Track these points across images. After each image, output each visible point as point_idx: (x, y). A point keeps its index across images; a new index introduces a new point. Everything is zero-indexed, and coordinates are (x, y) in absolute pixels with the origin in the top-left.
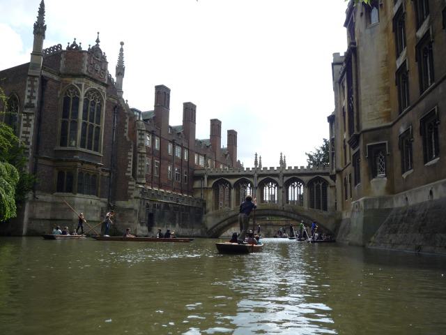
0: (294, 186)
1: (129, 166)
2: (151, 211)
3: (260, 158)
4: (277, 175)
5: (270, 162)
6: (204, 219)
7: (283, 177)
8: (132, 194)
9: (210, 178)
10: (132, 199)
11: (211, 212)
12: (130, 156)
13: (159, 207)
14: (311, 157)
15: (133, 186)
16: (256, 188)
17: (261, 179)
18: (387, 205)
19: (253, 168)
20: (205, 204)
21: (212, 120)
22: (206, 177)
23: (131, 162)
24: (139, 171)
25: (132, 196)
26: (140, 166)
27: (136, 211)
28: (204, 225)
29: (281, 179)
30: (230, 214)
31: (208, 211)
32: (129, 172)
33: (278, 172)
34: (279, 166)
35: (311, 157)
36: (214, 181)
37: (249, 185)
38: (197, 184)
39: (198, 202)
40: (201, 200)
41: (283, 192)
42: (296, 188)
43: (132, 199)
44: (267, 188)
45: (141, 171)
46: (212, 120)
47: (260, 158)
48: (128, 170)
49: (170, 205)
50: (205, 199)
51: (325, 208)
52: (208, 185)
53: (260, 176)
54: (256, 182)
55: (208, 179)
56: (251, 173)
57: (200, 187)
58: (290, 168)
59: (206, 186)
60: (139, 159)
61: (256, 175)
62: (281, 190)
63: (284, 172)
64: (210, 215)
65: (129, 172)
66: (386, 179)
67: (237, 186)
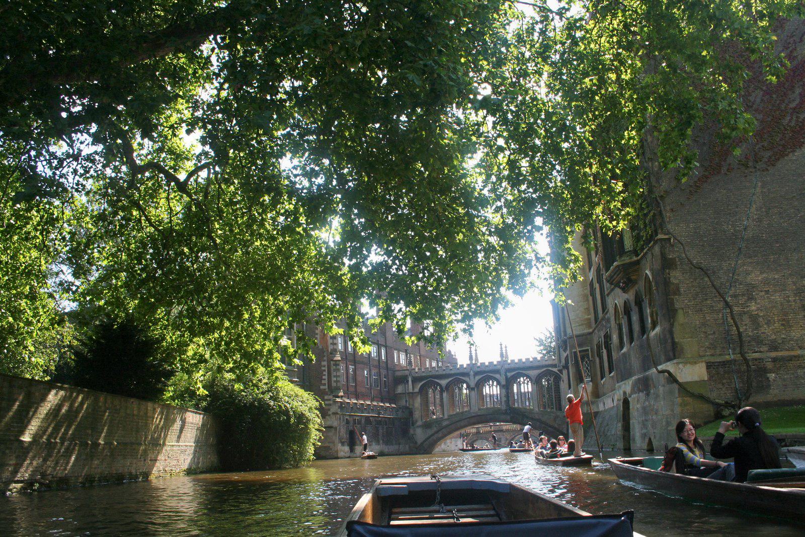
0: (519, 382)
1: (324, 377)
2: (351, 428)
6: (412, 432)
8: (329, 410)
9: (416, 380)
10: (329, 415)
12: (324, 366)
13: (359, 423)
14: (541, 343)
15: (330, 400)
17: (478, 378)
18: (594, 409)
19: (468, 365)
20: (411, 413)
23: (326, 373)
24: (334, 381)
25: (330, 413)
26: (334, 376)
27: (336, 428)
28: (412, 439)
30: (445, 424)
31: (417, 421)
32: (324, 385)
33: (499, 367)
35: (541, 343)
36: (421, 384)
37: (465, 386)
38: (400, 389)
39: (403, 412)
40: (407, 408)
43: (329, 415)
44: (487, 387)
45: (337, 382)
48: (323, 382)
49: (371, 418)
50: (411, 407)
52: (413, 389)
53: (476, 374)
56: (465, 371)
59: (411, 391)
60: (333, 368)
61: (472, 373)
63: (506, 366)
64: (418, 427)
65: (324, 385)
66: (591, 383)
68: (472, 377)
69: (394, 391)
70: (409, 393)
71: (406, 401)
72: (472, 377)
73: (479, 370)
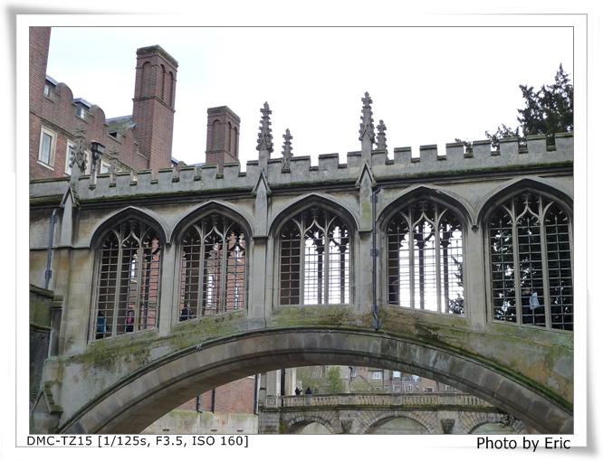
3: (288, 137)
4: (349, 186)
9: (85, 208)
16: (262, 241)
17: (281, 205)
22: (68, 207)
31: (70, 342)
33: (354, 172)
34: (357, 146)
41: (375, 253)
47: (288, 137)
50: (57, 293)
52: (75, 237)
53: (276, 192)
54: (260, 217)
55: (75, 211)
56: (242, 184)
57: (46, 246)
58: (403, 151)
59: (66, 240)
61: (262, 191)
63: (380, 170)
64: (73, 359)
67: (186, 236)
70: (59, 249)
71: (49, 274)
73: (286, 180)
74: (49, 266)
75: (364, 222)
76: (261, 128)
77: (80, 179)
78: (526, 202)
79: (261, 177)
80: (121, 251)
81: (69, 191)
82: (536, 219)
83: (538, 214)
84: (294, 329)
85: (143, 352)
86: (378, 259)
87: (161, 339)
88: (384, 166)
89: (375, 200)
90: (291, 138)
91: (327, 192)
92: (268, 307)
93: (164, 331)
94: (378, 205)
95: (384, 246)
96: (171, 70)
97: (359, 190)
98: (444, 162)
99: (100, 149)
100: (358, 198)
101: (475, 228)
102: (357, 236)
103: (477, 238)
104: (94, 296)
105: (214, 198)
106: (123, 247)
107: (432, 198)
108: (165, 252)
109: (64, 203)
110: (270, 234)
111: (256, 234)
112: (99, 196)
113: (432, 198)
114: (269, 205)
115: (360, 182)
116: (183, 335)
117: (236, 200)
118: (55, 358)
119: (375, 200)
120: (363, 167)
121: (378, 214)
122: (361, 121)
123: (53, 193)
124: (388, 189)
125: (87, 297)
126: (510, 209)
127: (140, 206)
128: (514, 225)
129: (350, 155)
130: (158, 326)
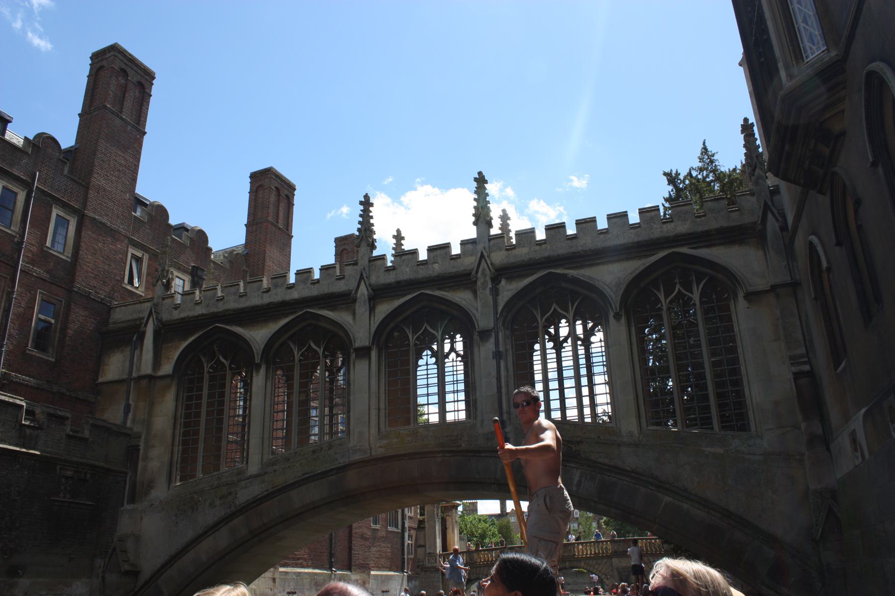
5: (426, 220)
6: (125, 525)
7: (496, 280)
9: (168, 332)
11: (160, 492)
16: (363, 353)
17: (384, 309)
20: (133, 454)
21: (254, 176)
29: (485, 293)
30: (244, 495)
31: (150, 485)
33: (470, 262)
34: (471, 233)
36: (185, 344)
38: (115, 367)
41: (498, 355)
42: (568, 347)
46: (254, 176)
50: (137, 429)
51: (735, 417)
54: (360, 326)
55: (157, 334)
57: (125, 377)
58: (526, 235)
59: (146, 368)
61: (363, 291)
62: (489, 346)
63: (499, 258)
68: (362, 308)
69: (97, 372)
70: (141, 378)
72: (362, 308)
74: (128, 399)
75: (484, 320)
76: (360, 223)
77: (163, 299)
78: (677, 280)
79: (361, 277)
80: (206, 376)
81: (150, 313)
82: (690, 299)
83: (692, 293)
84: (404, 455)
85: (230, 494)
86: (502, 363)
87: (250, 477)
88: (504, 253)
89: (495, 292)
90: (403, 238)
91: (439, 289)
92: (374, 430)
93: (253, 468)
94: (500, 298)
95: (509, 347)
96: (286, 192)
97: (476, 281)
98: (574, 241)
99: (199, 273)
100: (475, 293)
101: (617, 317)
102: (476, 337)
103: (620, 328)
104: (177, 432)
105: (309, 307)
106: (209, 372)
107: (564, 285)
108: (254, 374)
109: (146, 326)
110: (373, 343)
111: (357, 344)
112: (183, 315)
113: (564, 285)
114: (372, 310)
115: (477, 272)
116: (275, 471)
117: (333, 308)
118: (131, 507)
119: (495, 292)
120: (479, 255)
121: (500, 308)
122: (475, 204)
123: (135, 316)
124: (510, 279)
125: (169, 432)
126: (659, 290)
127: (227, 324)
128: (664, 308)
129: (464, 243)
130: (247, 463)
